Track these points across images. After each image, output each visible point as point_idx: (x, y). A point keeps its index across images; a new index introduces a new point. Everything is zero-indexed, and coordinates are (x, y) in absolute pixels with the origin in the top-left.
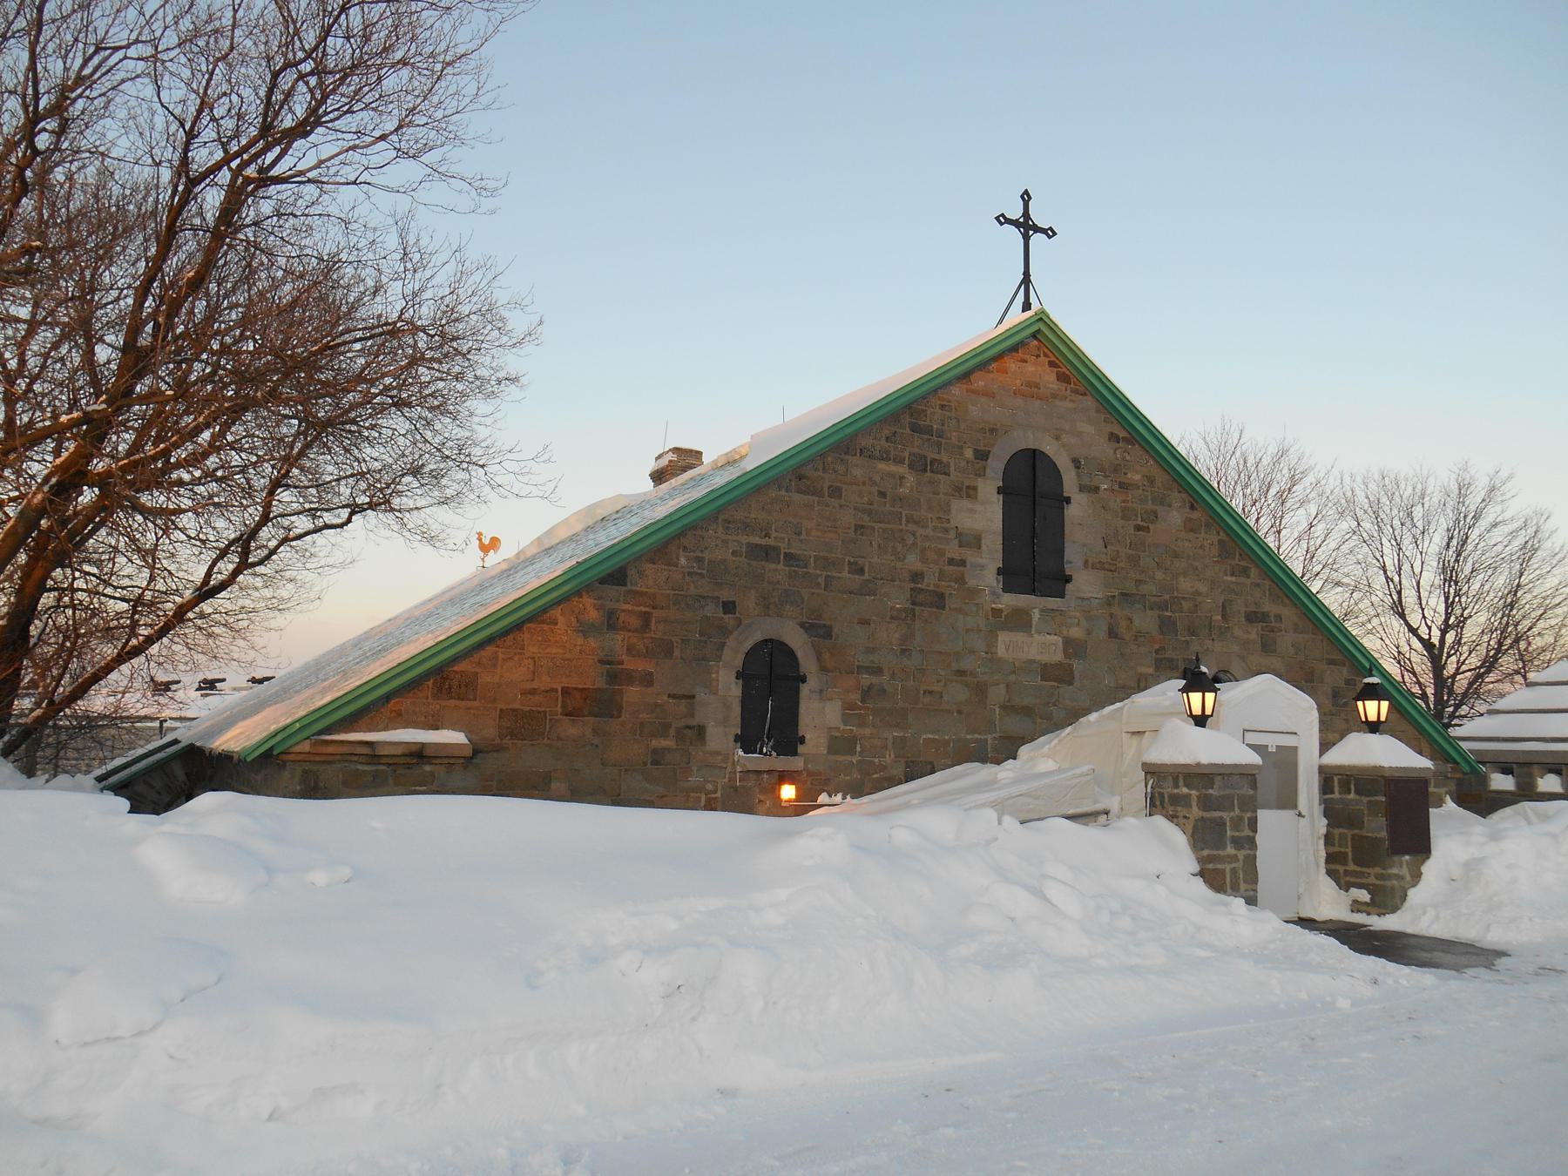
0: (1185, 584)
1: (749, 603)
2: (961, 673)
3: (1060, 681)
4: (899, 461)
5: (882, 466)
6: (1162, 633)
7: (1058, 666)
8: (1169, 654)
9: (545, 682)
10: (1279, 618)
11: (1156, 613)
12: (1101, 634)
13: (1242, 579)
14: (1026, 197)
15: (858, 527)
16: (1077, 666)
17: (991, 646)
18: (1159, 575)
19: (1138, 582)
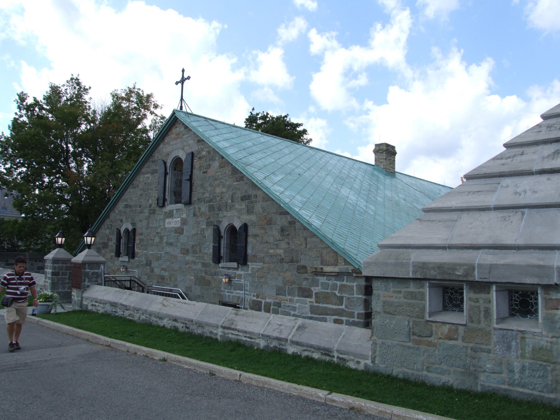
0: (218, 190)
1: (124, 220)
2: (158, 233)
3: (180, 233)
4: (149, 173)
5: (146, 176)
6: (210, 212)
7: (179, 228)
8: (212, 219)
9: (101, 241)
10: (256, 196)
11: (207, 204)
12: (192, 215)
13: (241, 182)
14: (183, 71)
15: (141, 194)
16: (185, 227)
17: (164, 224)
18: (209, 189)
19: (203, 193)
